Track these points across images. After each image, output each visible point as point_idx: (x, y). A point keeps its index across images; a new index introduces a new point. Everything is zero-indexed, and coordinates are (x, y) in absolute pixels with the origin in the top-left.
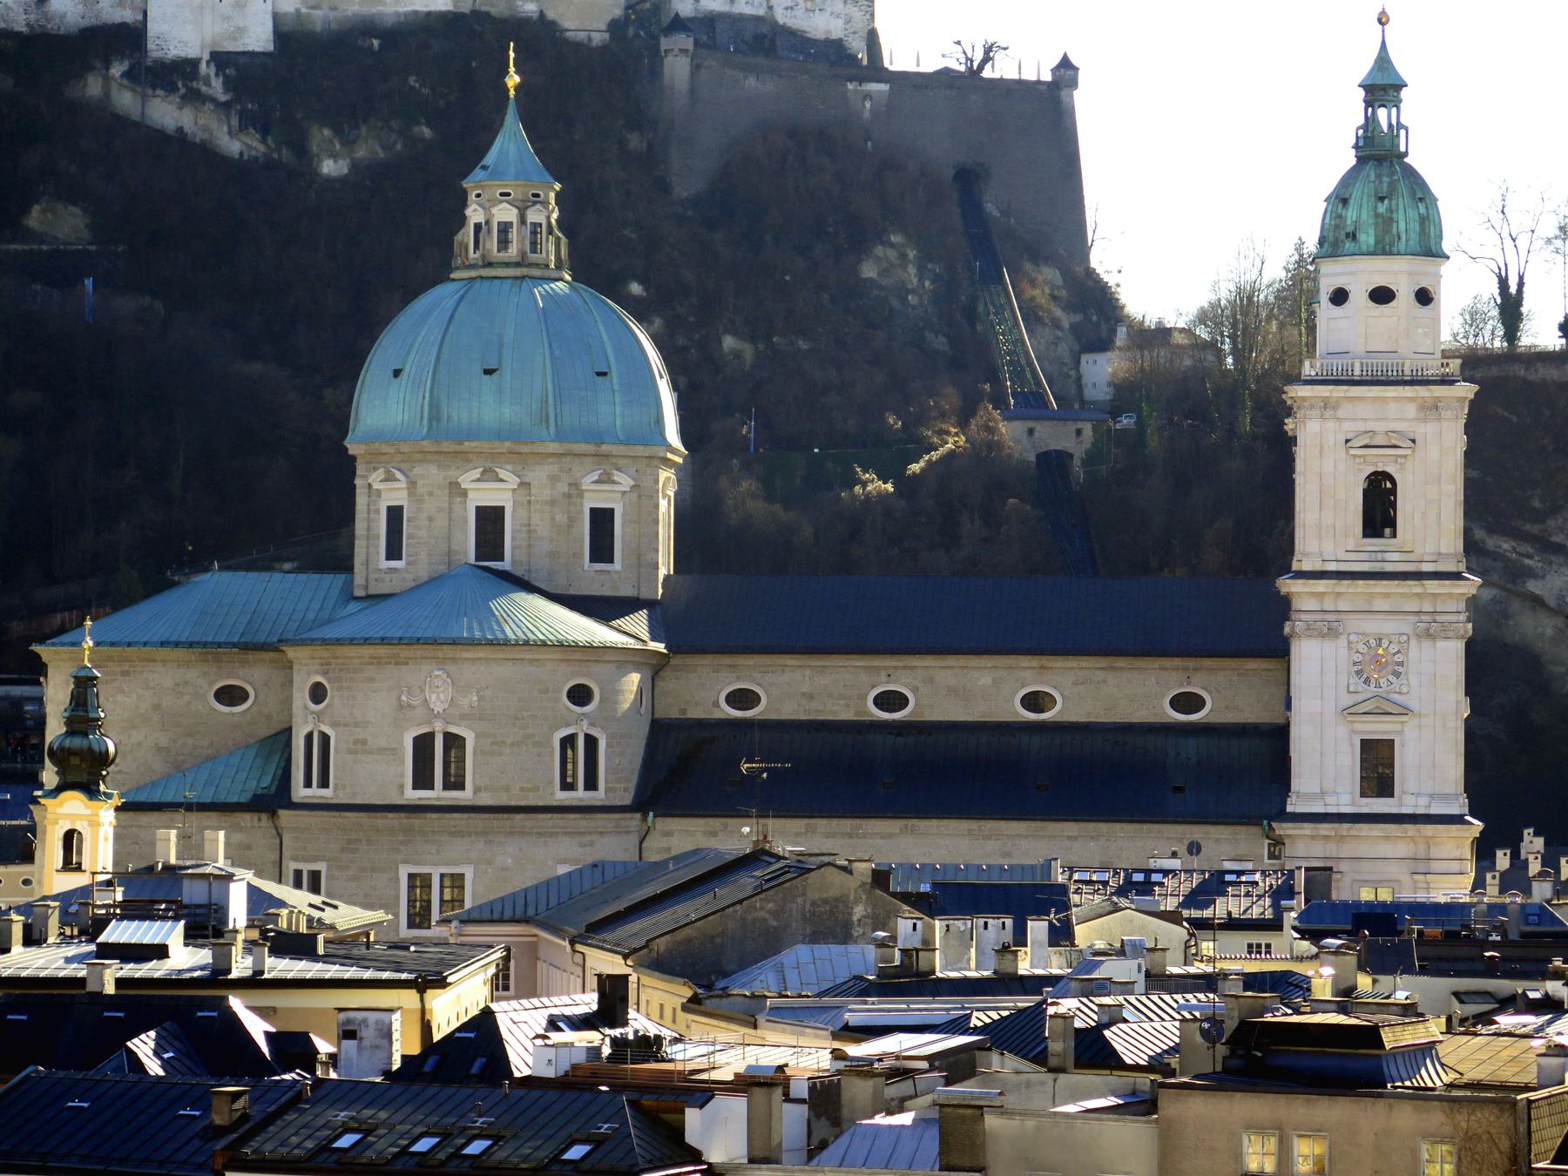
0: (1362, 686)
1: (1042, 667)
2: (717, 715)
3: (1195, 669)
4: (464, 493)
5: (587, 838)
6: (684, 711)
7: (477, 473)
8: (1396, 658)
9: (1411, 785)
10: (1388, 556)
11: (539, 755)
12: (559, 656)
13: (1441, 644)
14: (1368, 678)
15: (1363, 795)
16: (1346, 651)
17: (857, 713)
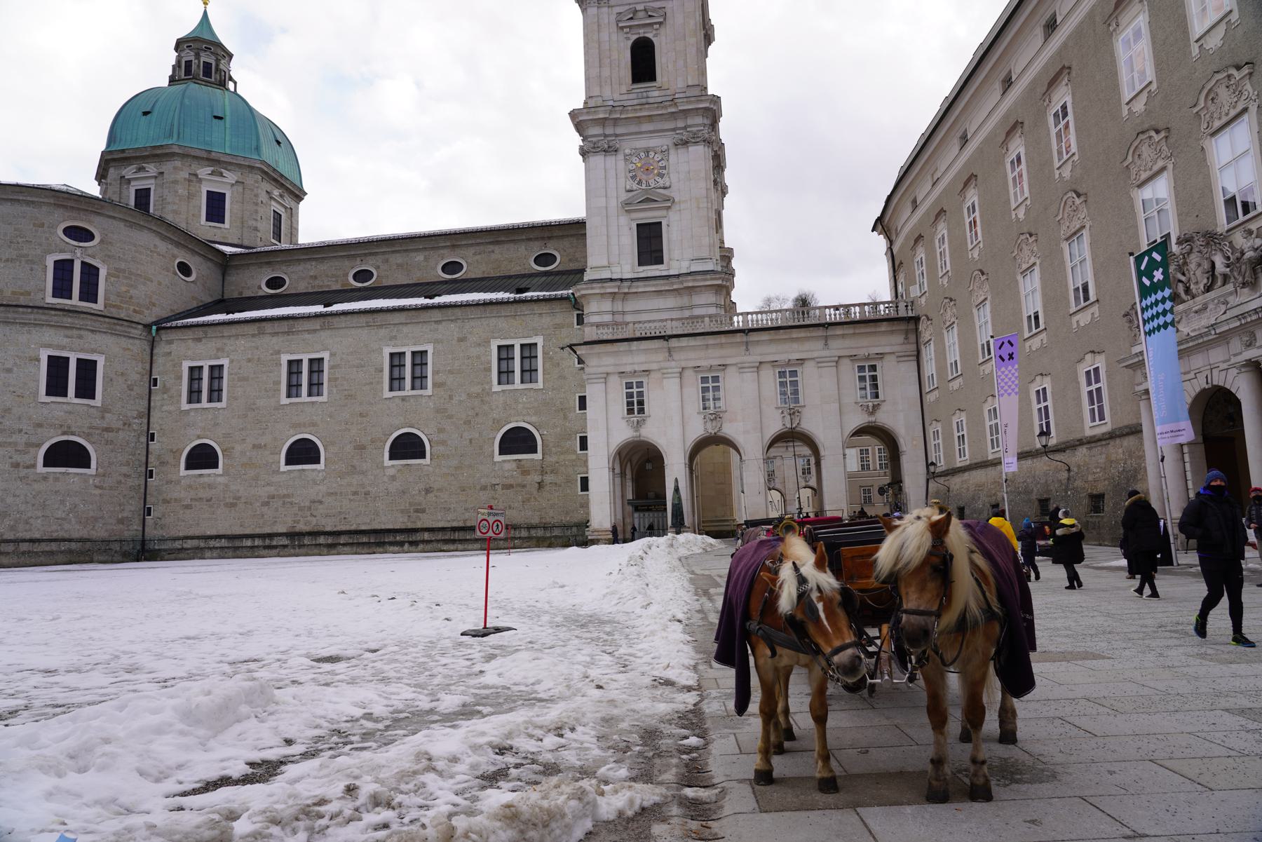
0: (635, 186)
1: (454, 247)
2: (260, 293)
3: (549, 238)
4: (129, 181)
5: (75, 332)
6: (241, 293)
7: (133, 168)
8: (660, 164)
9: (676, 254)
10: (651, 94)
11: (32, 270)
12: (52, 201)
13: (692, 149)
14: (640, 180)
15: (640, 264)
16: (623, 162)
17: (342, 285)
